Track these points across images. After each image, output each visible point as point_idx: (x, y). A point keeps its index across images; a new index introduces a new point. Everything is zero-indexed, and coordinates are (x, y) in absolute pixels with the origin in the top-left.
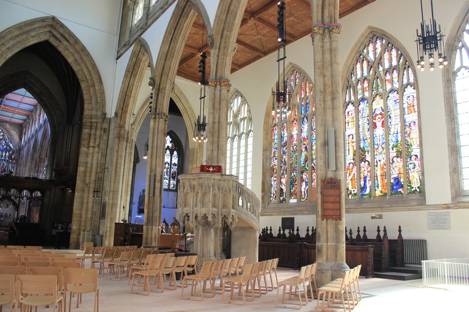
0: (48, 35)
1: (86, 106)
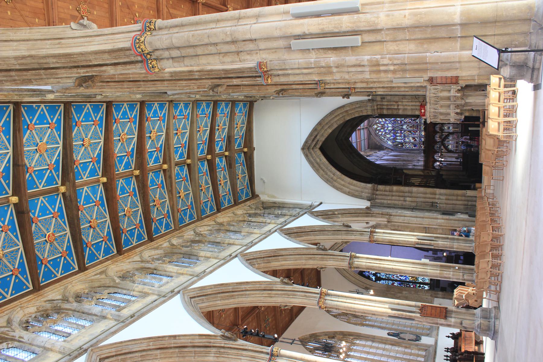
0: (315, 150)
1: (365, 114)
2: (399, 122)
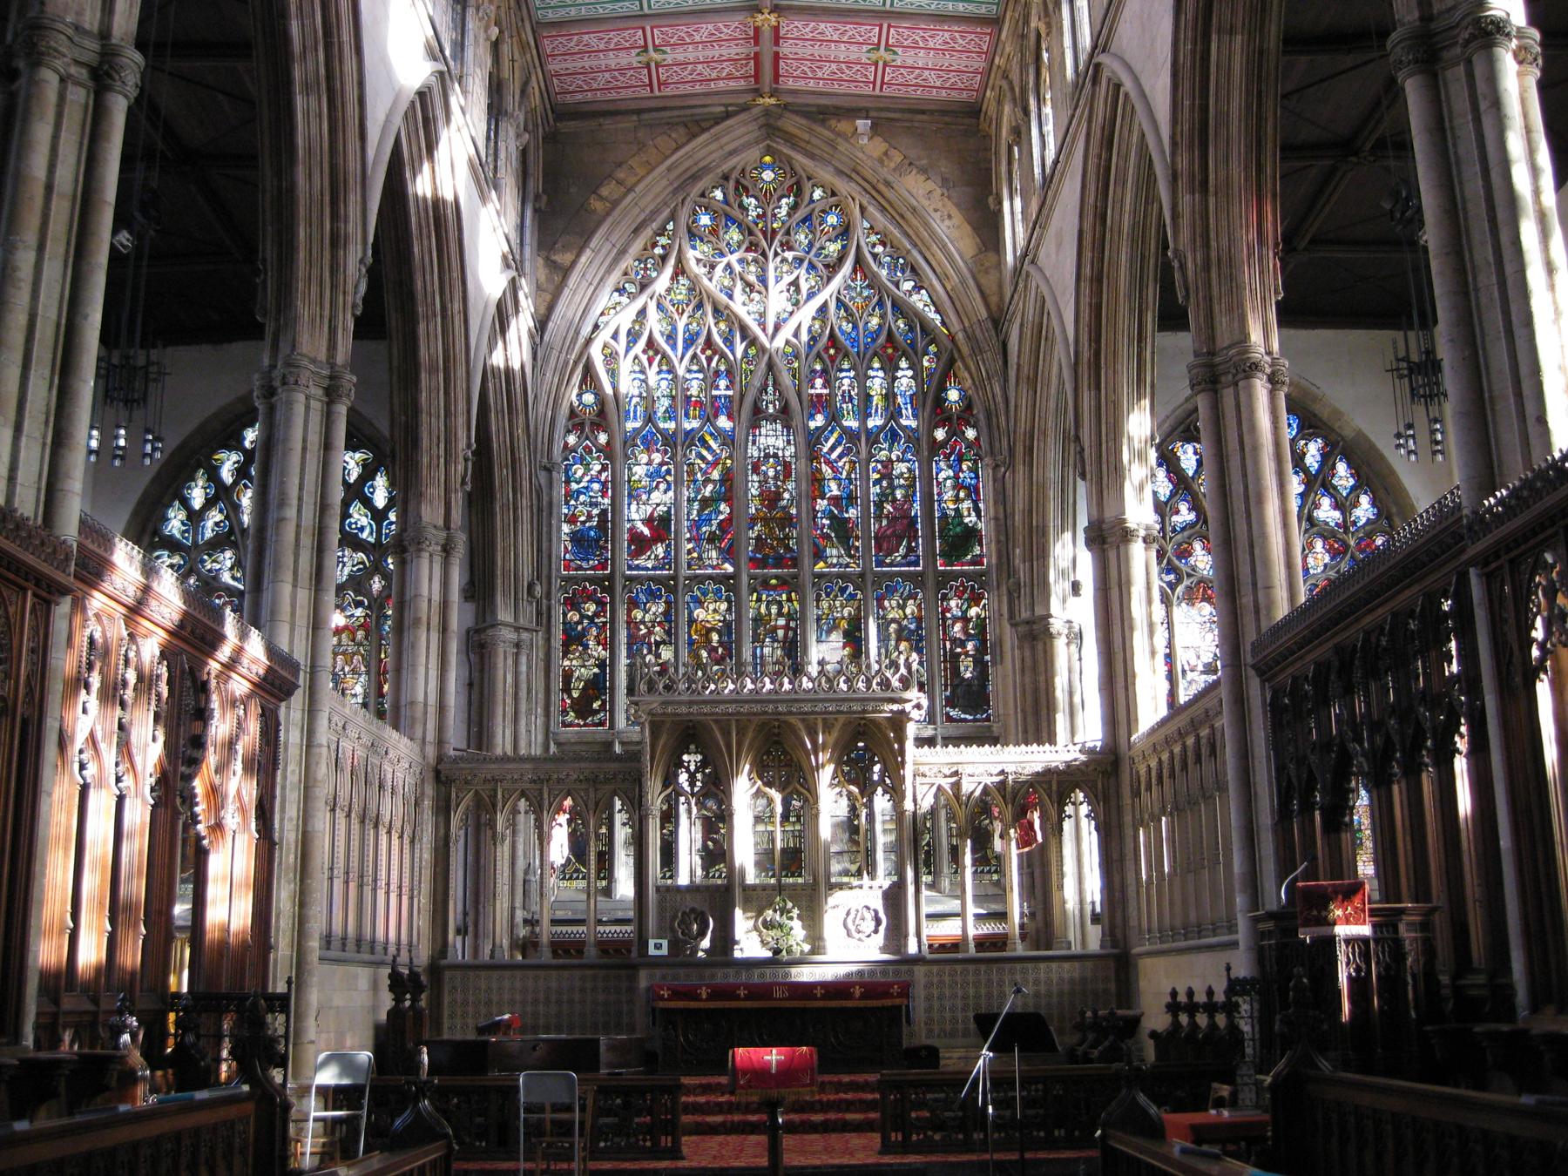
2: (819, 386)
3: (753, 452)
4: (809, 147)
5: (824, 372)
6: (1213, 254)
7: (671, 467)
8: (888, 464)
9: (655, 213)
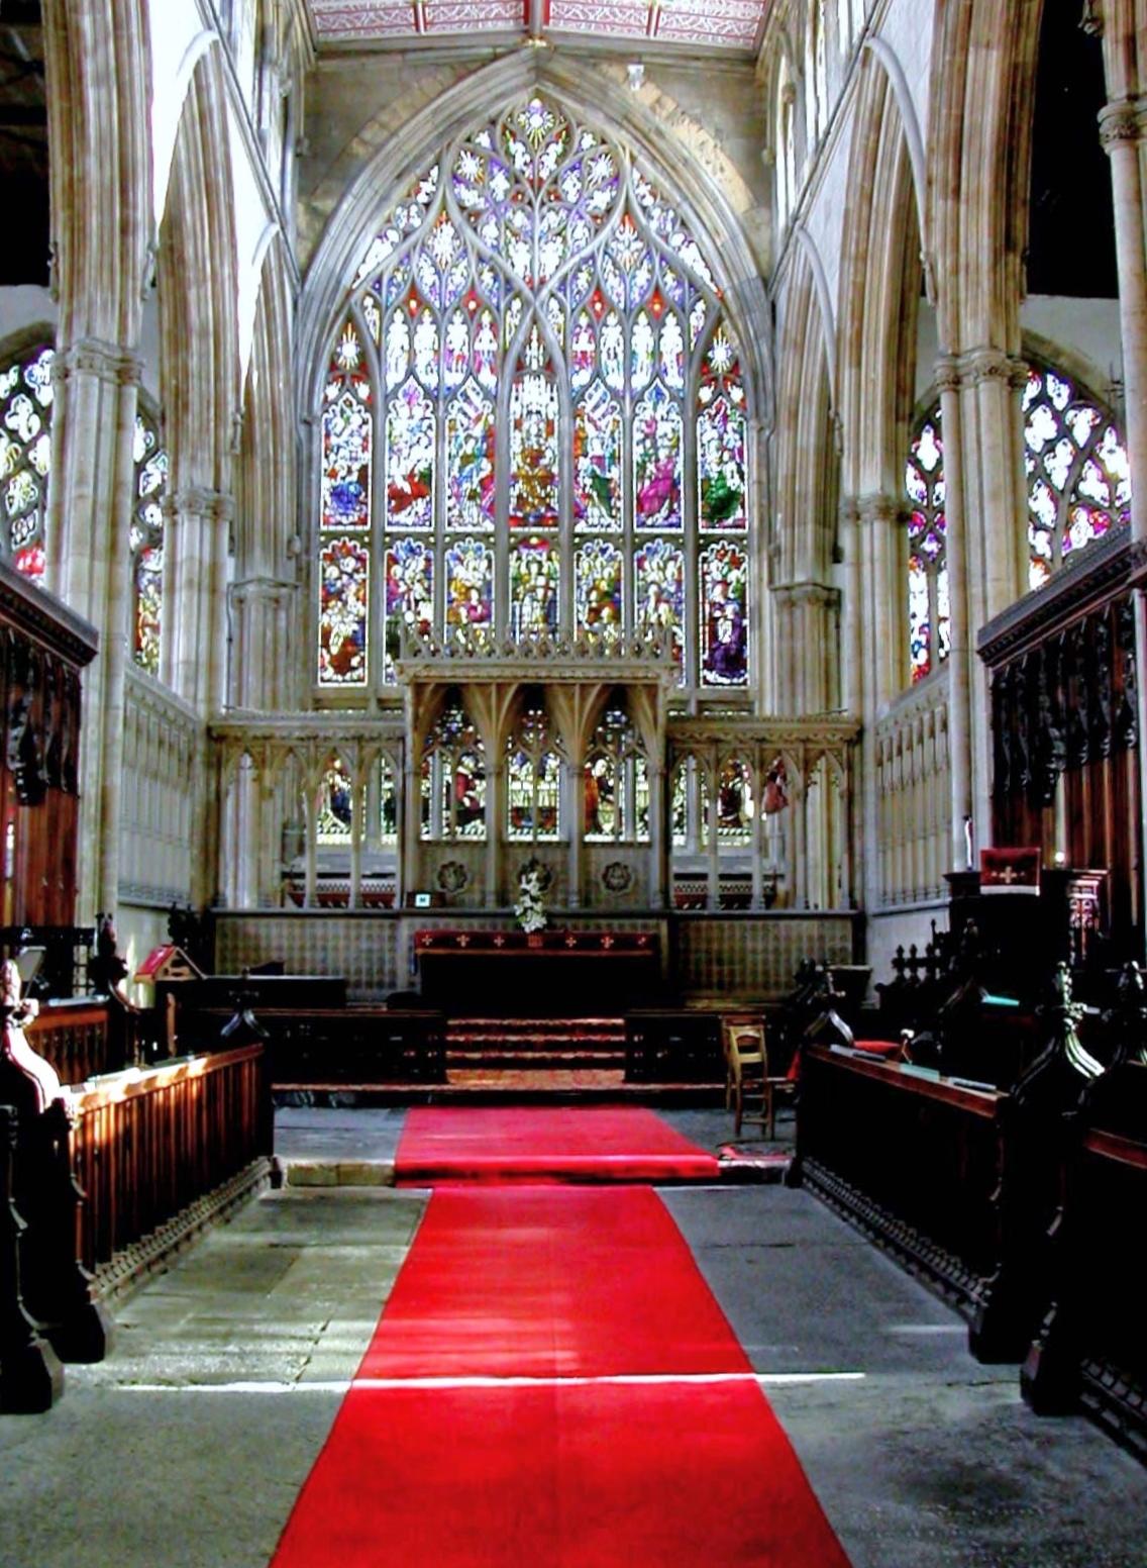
2: (583, 344)
3: (515, 407)
4: (579, 91)
5: (590, 326)
6: (962, 260)
7: (433, 422)
8: (652, 423)
9: (419, 158)
